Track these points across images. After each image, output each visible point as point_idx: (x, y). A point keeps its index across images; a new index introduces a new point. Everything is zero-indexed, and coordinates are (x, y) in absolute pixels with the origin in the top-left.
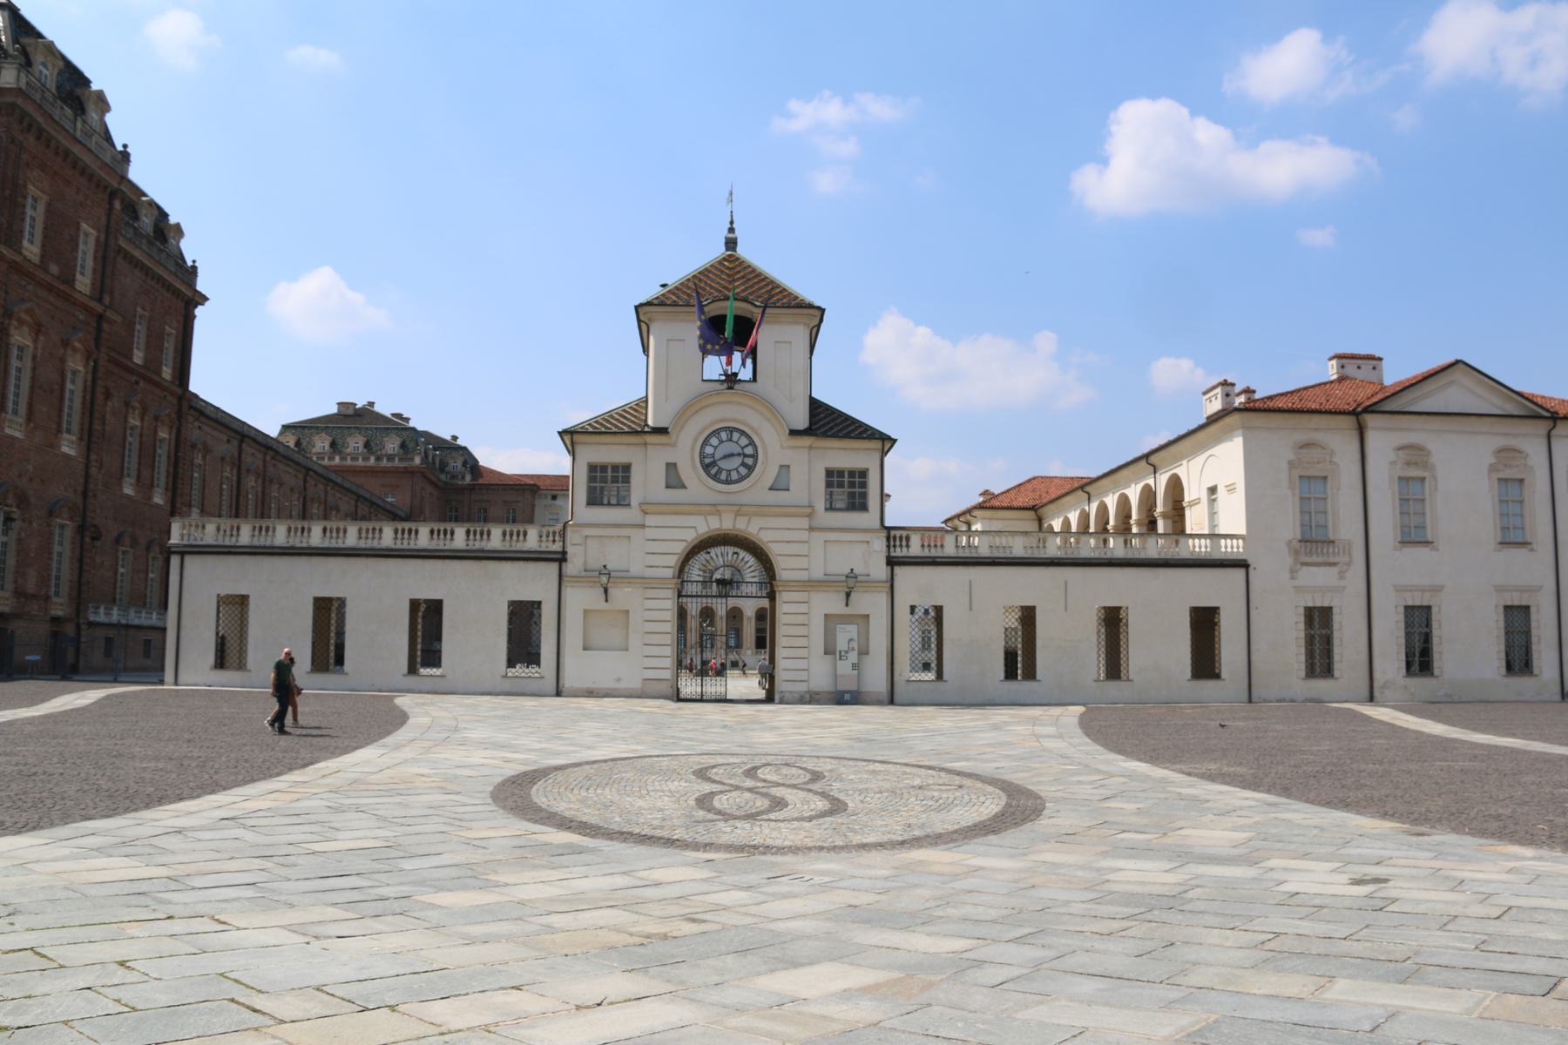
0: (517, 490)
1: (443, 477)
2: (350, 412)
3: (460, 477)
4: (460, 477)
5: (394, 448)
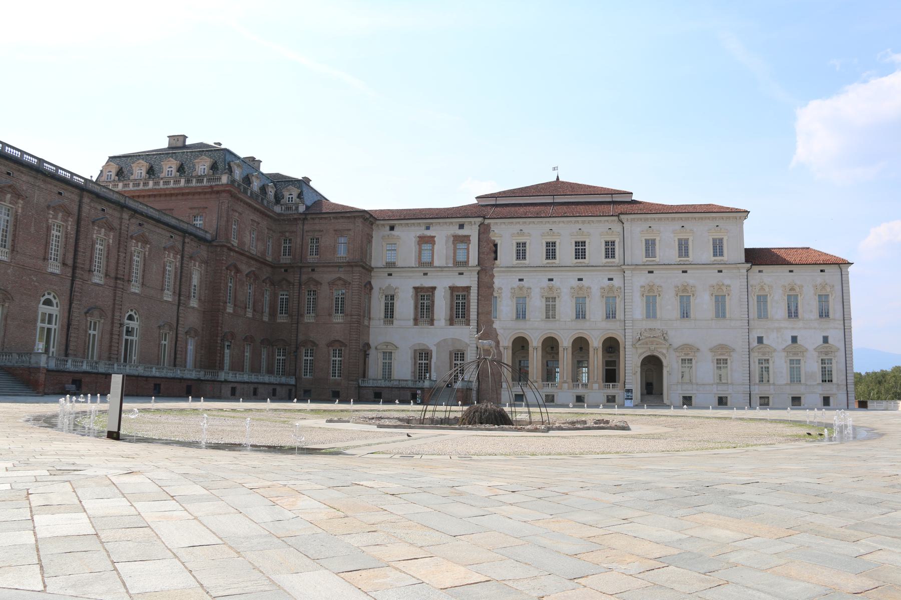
1: (277, 209)
2: (180, 144)
3: (294, 208)
4: (294, 208)
5: (204, 169)
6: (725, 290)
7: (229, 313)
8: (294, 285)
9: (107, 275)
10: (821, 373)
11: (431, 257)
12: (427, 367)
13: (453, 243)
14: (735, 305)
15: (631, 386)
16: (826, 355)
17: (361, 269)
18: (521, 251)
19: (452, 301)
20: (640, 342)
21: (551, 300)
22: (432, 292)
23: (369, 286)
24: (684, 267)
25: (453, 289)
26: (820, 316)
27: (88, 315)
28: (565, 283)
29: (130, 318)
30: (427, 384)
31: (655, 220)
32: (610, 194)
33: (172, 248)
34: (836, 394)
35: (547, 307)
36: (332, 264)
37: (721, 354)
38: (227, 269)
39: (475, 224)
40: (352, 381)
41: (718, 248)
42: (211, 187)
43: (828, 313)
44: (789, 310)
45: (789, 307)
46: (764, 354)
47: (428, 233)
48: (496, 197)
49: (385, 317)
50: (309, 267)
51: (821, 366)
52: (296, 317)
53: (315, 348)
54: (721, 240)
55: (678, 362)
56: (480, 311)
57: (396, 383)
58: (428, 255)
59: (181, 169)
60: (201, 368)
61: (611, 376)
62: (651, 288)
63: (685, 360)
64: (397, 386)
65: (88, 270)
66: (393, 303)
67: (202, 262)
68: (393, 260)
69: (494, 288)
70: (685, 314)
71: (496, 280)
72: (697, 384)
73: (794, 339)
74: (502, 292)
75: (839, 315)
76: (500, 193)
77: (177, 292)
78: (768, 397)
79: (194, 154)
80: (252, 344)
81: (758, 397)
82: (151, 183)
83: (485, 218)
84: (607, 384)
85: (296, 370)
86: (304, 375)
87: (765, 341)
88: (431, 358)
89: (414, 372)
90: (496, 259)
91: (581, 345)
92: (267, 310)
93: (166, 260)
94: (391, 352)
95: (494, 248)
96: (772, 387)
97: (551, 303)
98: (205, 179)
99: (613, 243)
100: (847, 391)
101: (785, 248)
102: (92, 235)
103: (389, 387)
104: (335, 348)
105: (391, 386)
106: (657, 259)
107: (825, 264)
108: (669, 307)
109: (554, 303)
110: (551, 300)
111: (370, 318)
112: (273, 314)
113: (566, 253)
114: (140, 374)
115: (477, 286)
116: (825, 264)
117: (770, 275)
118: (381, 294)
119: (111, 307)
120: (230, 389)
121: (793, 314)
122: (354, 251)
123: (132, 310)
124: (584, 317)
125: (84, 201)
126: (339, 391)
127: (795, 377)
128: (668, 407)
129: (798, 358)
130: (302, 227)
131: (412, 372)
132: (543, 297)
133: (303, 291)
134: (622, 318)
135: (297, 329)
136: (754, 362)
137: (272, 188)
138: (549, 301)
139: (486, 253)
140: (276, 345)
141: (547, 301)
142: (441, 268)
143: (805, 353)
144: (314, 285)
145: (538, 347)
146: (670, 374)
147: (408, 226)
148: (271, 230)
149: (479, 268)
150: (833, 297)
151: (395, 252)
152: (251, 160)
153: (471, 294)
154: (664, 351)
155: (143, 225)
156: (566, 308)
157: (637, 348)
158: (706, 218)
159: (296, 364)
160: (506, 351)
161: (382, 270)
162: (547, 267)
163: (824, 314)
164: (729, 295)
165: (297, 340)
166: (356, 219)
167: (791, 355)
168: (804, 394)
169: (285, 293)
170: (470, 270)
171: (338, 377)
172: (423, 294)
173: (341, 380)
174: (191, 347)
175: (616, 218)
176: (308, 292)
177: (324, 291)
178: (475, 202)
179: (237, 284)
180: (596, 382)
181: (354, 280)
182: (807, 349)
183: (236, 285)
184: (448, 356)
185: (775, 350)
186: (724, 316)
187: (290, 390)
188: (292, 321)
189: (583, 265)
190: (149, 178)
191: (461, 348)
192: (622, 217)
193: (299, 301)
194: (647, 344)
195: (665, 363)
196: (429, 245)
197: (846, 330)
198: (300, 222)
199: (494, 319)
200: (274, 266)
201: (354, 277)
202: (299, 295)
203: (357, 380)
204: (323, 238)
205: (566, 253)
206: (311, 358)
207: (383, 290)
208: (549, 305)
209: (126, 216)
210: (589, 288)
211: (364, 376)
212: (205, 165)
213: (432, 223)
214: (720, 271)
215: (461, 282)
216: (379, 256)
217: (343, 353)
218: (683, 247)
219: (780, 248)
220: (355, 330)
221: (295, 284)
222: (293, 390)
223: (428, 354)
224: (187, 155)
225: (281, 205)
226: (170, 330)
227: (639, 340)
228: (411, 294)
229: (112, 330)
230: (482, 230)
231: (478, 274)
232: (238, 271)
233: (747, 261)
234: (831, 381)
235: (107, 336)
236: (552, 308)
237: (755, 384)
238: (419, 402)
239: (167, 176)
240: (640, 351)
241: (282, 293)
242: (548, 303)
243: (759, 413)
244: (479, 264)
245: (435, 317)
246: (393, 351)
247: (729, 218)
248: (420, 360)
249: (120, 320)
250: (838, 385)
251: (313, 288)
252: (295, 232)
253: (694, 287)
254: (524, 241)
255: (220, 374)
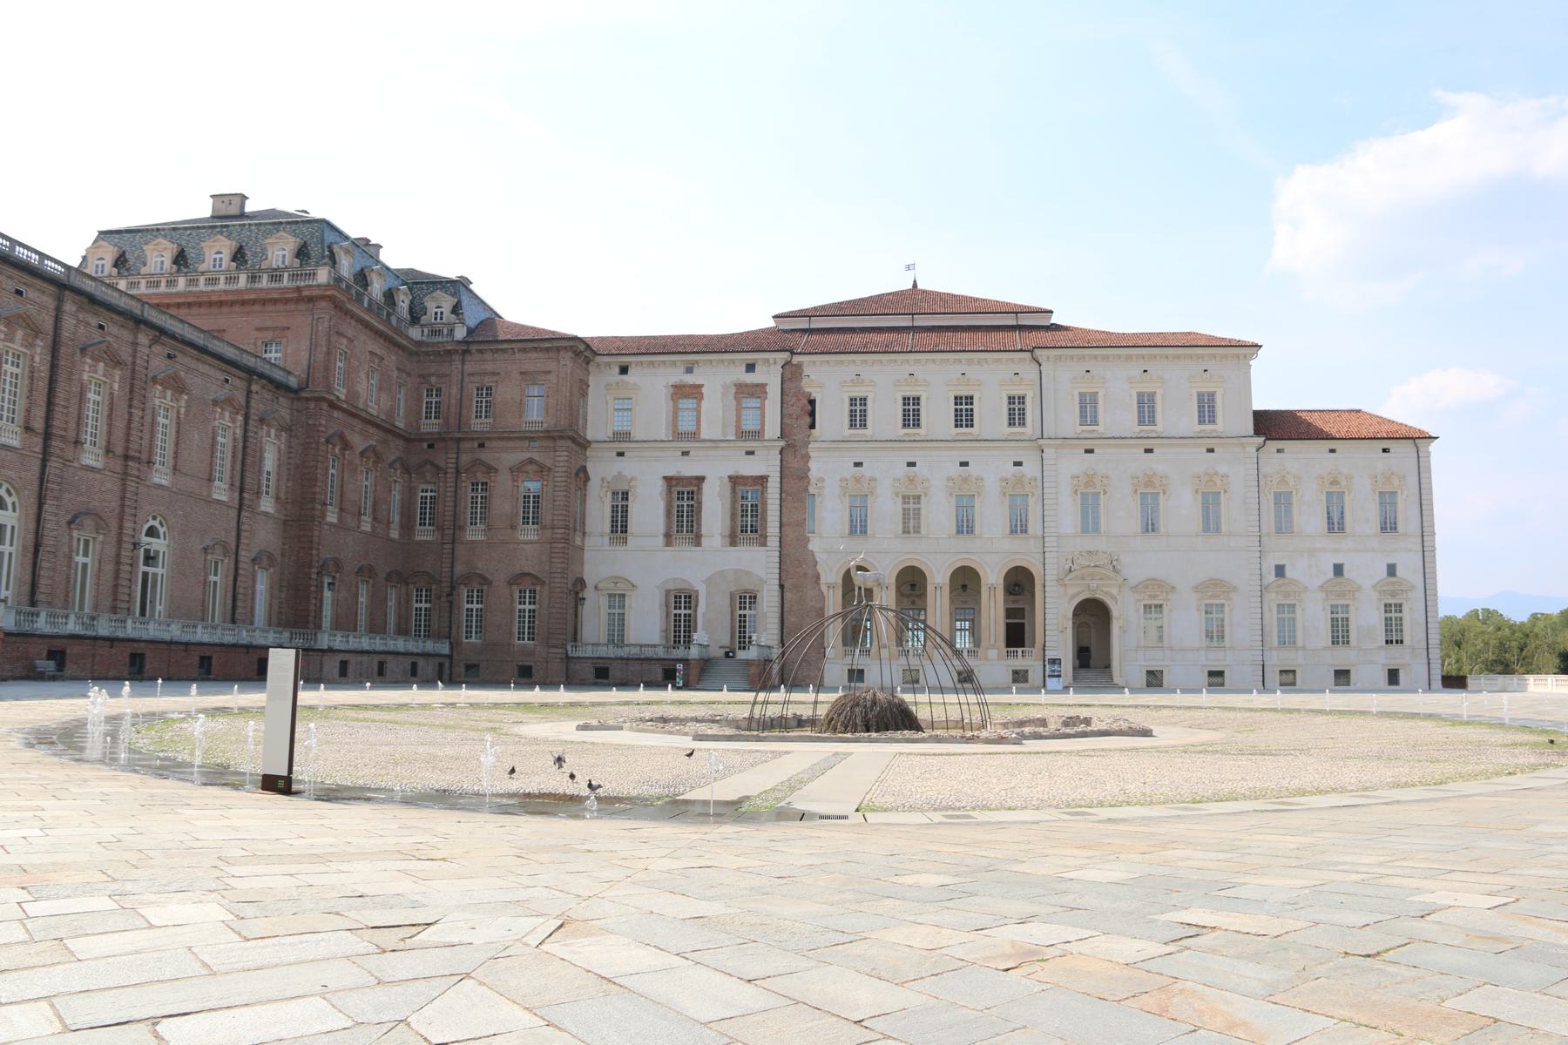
0: (547, 350)
1: (415, 333)
2: (234, 210)
3: (445, 331)
4: (445, 331)
5: (284, 256)
6: (1218, 482)
7: (331, 525)
8: (446, 473)
9: (108, 451)
10: (1384, 628)
11: (694, 423)
12: (689, 621)
13: (736, 398)
14: (1234, 512)
15: (1055, 653)
16: (1392, 596)
17: (569, 443)
18: (858, 414)
19: (734, 502)
20: (1072, 575)
21: (912, 501)
22: (698, 486)
23: (582, 475)
24: (1149, 444)
25: (736, 481)
26: (1382, 529)
27: (72, 526)
28: (938, 469)
29: (152, 532)
30: (694, 652)
31: (1096, 358)
32: (1013, 313)
33: (229, 401)
34: (1409, 665)
35: (905, 512)
36: (516, 435)
37: (1212, 597)
38: (327, 442)
39: (775, 363)
40: (556, 647)
41: (1206, 408)
42: (298, 289)
43: (1395, 523)
44: (1328, 518)
45: (1328, 513)
46: (1287, 595)
47: (690, 379)
48: (810, 317)
49: (612, 532)
50: (473, 439)
51: (1383, 615)
52: (451, 532)
53: (485, 587)
54: (1212, 396)
55: (1137, 611)
56: (784, 519)
57: (635, 651)
58: (690, 418)
59: (239, 256)
60: (279, 625)
61: (1016, 636)
62: (1090, 479)
63: (1150, 606)
64: (636, 657)
65: (74, 440)
66: (627, 506)
67: (281, 429)
68: (625, 428)
69: (809, 480)
70: (1150, 527)
71: (812, 465)
72: (1171, 649)
73: (1338, 570)
74: (823, 487)
75: (1414, 527)
76: (815, 309)
77: (237, 484)
78: (1294, 672)
79: (262, 228)
80: (371, 581)
81: (1277, 670)
82: (182, 282)
83: (793, 353)
84: (1009, 649)
85: (450, 628)
86: (467, 638)
87: (1289, 573)
88: (697, 605)
89: (666, 631)
90: (812, 426)
91: (965, 582)
92: (396, 518)
93: (217, 423)
94: (624, 595)
95: (810, 408)
96: (1300, 653)
97: (911, 506)
98: (286, 275)
99: (1022, 399)
100: (1429, 659)
101: (1320, 411)
102: (81, 375)
103: (622, 659)
104: (522, 588)
105: (625, 656)
106: (1100, 428)
107: (1390, 438)
108: (1121, 513)
109: (916, 506)
110: (912, 501)
111: (584, 533)
112: (407, 527)
113: (938, 416)
114: (175, 639)
115: (779, 475)
116: (1390, 438)
117: (1296, 456)
118: (604, 490)
119: (117, 511)
120: (338, 664)
121: (1335, 525)
122: (557, 410)
123: (154, 518)
124: (971, 531)
125: (64, 308)
126: (531, 667)
127: (1340, 633)
128: (1119, 689)
129: (1344, 602)
130: (460, 367)
131: (662, 631)
132: (897, 495)
133: (463, 484)
134: (1039, 533)
135: (453, 553)
136: (1270, 610)
137: (406, 294)
138: (909, 503)
139: (795, 416)
140: (414, 583)
141: (904, 503)
142: (715, 443)
143: (1357, 594)
144: (484, 473)
145: (943, 584)
146: (1124, 632)
147: (676, 366)
148: (403, 371)
149: (782, 443)
150: (1404, 497)
151: (630, 413)
152: (363, 242)
153: (769, 490)
154: (1114, 591)
155: (175, 357)
156: (938, 514)
157: (1065, 585)
158: (1186, 356)
159: (450, 617)
160: (831, 591)
161: (605, 445)
162: (904, 441)
163: (1389, 526)
164: (1225, 492)
165: (452, 572)
166: (561, 353)
167: (1333, 597)
168: (1354, 665)
169: (429, 487)
170: (766, 446)
171: (529, 639)
172: (681, 489)
173: (535, 645)
174: (262, 586)
175: (1028, 355)
176: (473, 485)
177: (502, 482)
178: (771, 324)
179: (345, 469)
180: (993, 647)
181: (557, 464)
182: (1360, 587)
183: (343, 472)
184: (728, 601)
185: (1306, 589)
186: (1218, 530)
187: (441, 665)
188: (442, 539)
189: (970, 437)
190: (179, 271)
191: (751, 587)
192: (1038, 352)
193: (455, 501)
194: (1083, 579)
195: (1115, 611)
196: (690, 401)
197: (1426, 554)
198: (457, 357)
199: (810, 535)
200: (409, 439)
201: (558, 459)
202: (456, 492)
203: (564, 646)
204: (499, 386)
205: (938, 416)
206: (480, 606)
207: (608, 482)
208: (909, 509)
209: (143, 339)
210: (980, 479)
211: (575, 639)
212: (284, 250)
213: (697, 362)
214: (1211, 450)
215: (751, 468)
216: (599, 422)
217: (537, 596)
218: (1146, 408)
219: (1311, 411)
220: (561, 555)
221: (449, 470)
222: (447, 665)
223: (690, 597)
224: (250, 231)
225: (422, 326)
226: (225, 556)
227: (1070, 571)
228: (660, 489)
229: (118, 555)
230: (788, 375)
231: (781, 453)
232: (346, 445)
233: (1257, 432)
234: (1402, 642)
235: (109, 567)
236: (914, 514)
237: (1271, 649)
238: (681, 685)
239: (212, 269)
240: (1071, 591)
241: (424, 487)
242: (906, 506)
243: (1280, 699)
244: (782, 436)
245: (704, 531)
246: (627, 593)
247: (1225, 356)
248: (675, 608)
249: (133, 537)
250: (1413, 649)
251: (481, 477)
252: (447, 375)
253: (1167, 477)
254: (862, 395)
255: (319, 636)
